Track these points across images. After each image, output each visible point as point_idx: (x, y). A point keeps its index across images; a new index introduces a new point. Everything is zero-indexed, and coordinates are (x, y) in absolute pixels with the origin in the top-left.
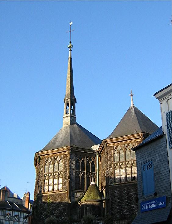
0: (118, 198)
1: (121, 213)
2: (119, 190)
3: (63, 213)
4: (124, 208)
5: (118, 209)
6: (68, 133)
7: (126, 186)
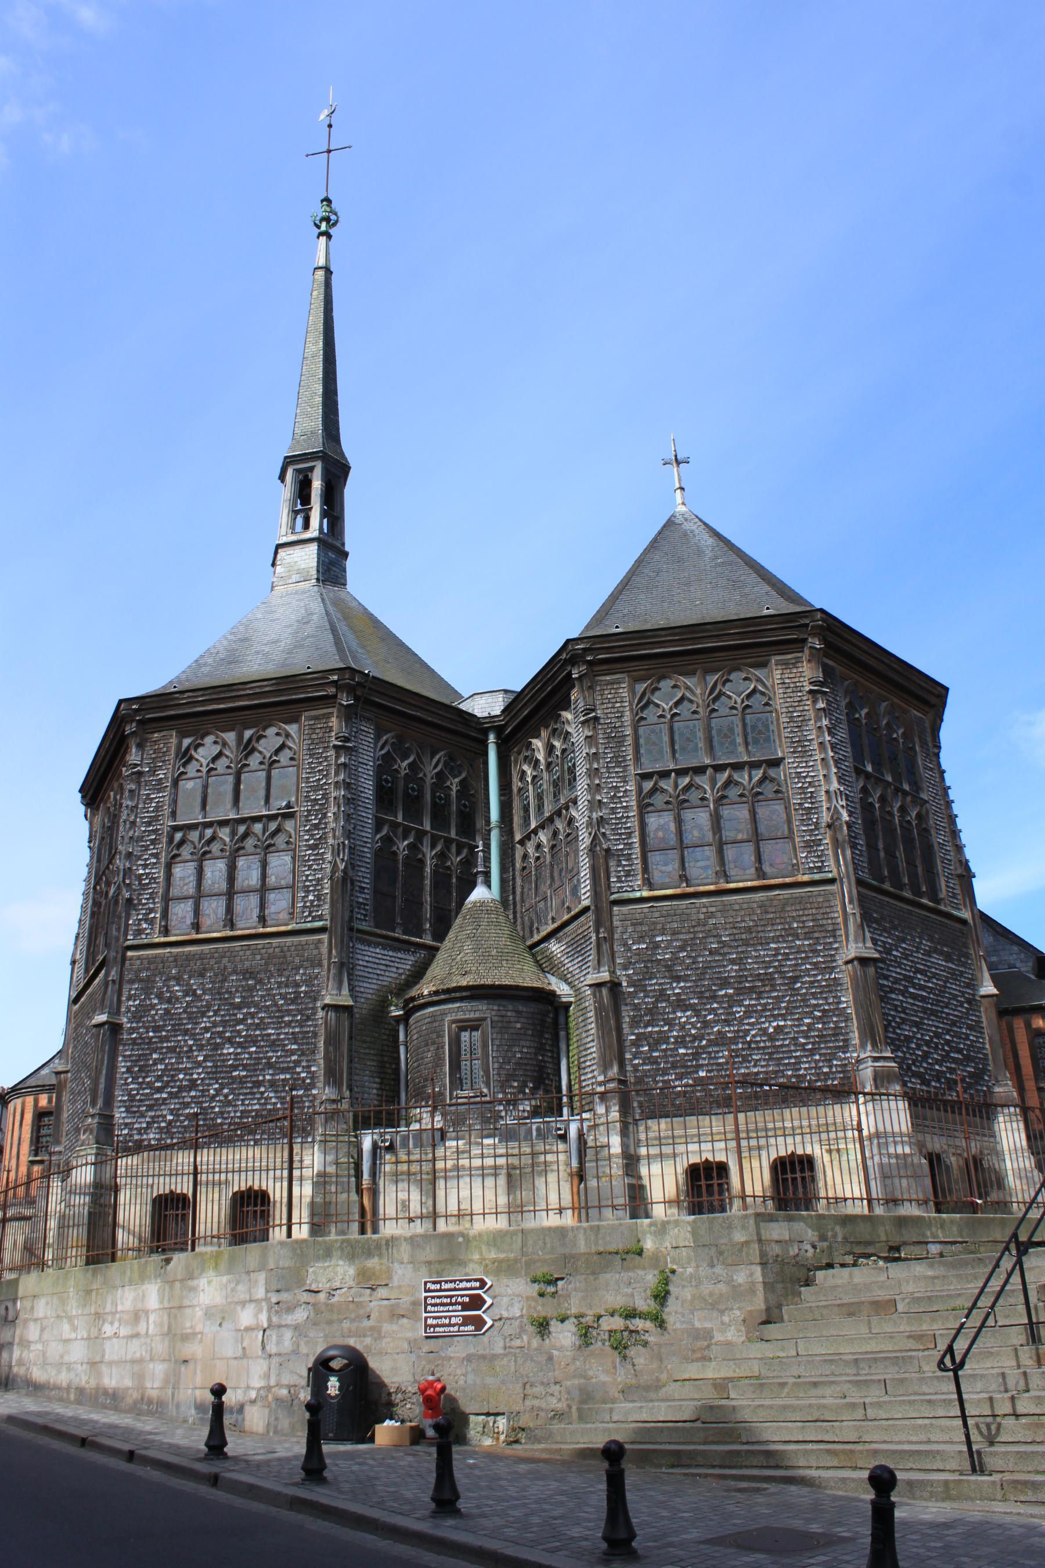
0: (678, 979)
1: (700, 1067)
2: (674, 933)
3: (297, 1063)
4: (721, 1040)
5: (681, 1042)
6: (315, 617)
7: (724, 910)
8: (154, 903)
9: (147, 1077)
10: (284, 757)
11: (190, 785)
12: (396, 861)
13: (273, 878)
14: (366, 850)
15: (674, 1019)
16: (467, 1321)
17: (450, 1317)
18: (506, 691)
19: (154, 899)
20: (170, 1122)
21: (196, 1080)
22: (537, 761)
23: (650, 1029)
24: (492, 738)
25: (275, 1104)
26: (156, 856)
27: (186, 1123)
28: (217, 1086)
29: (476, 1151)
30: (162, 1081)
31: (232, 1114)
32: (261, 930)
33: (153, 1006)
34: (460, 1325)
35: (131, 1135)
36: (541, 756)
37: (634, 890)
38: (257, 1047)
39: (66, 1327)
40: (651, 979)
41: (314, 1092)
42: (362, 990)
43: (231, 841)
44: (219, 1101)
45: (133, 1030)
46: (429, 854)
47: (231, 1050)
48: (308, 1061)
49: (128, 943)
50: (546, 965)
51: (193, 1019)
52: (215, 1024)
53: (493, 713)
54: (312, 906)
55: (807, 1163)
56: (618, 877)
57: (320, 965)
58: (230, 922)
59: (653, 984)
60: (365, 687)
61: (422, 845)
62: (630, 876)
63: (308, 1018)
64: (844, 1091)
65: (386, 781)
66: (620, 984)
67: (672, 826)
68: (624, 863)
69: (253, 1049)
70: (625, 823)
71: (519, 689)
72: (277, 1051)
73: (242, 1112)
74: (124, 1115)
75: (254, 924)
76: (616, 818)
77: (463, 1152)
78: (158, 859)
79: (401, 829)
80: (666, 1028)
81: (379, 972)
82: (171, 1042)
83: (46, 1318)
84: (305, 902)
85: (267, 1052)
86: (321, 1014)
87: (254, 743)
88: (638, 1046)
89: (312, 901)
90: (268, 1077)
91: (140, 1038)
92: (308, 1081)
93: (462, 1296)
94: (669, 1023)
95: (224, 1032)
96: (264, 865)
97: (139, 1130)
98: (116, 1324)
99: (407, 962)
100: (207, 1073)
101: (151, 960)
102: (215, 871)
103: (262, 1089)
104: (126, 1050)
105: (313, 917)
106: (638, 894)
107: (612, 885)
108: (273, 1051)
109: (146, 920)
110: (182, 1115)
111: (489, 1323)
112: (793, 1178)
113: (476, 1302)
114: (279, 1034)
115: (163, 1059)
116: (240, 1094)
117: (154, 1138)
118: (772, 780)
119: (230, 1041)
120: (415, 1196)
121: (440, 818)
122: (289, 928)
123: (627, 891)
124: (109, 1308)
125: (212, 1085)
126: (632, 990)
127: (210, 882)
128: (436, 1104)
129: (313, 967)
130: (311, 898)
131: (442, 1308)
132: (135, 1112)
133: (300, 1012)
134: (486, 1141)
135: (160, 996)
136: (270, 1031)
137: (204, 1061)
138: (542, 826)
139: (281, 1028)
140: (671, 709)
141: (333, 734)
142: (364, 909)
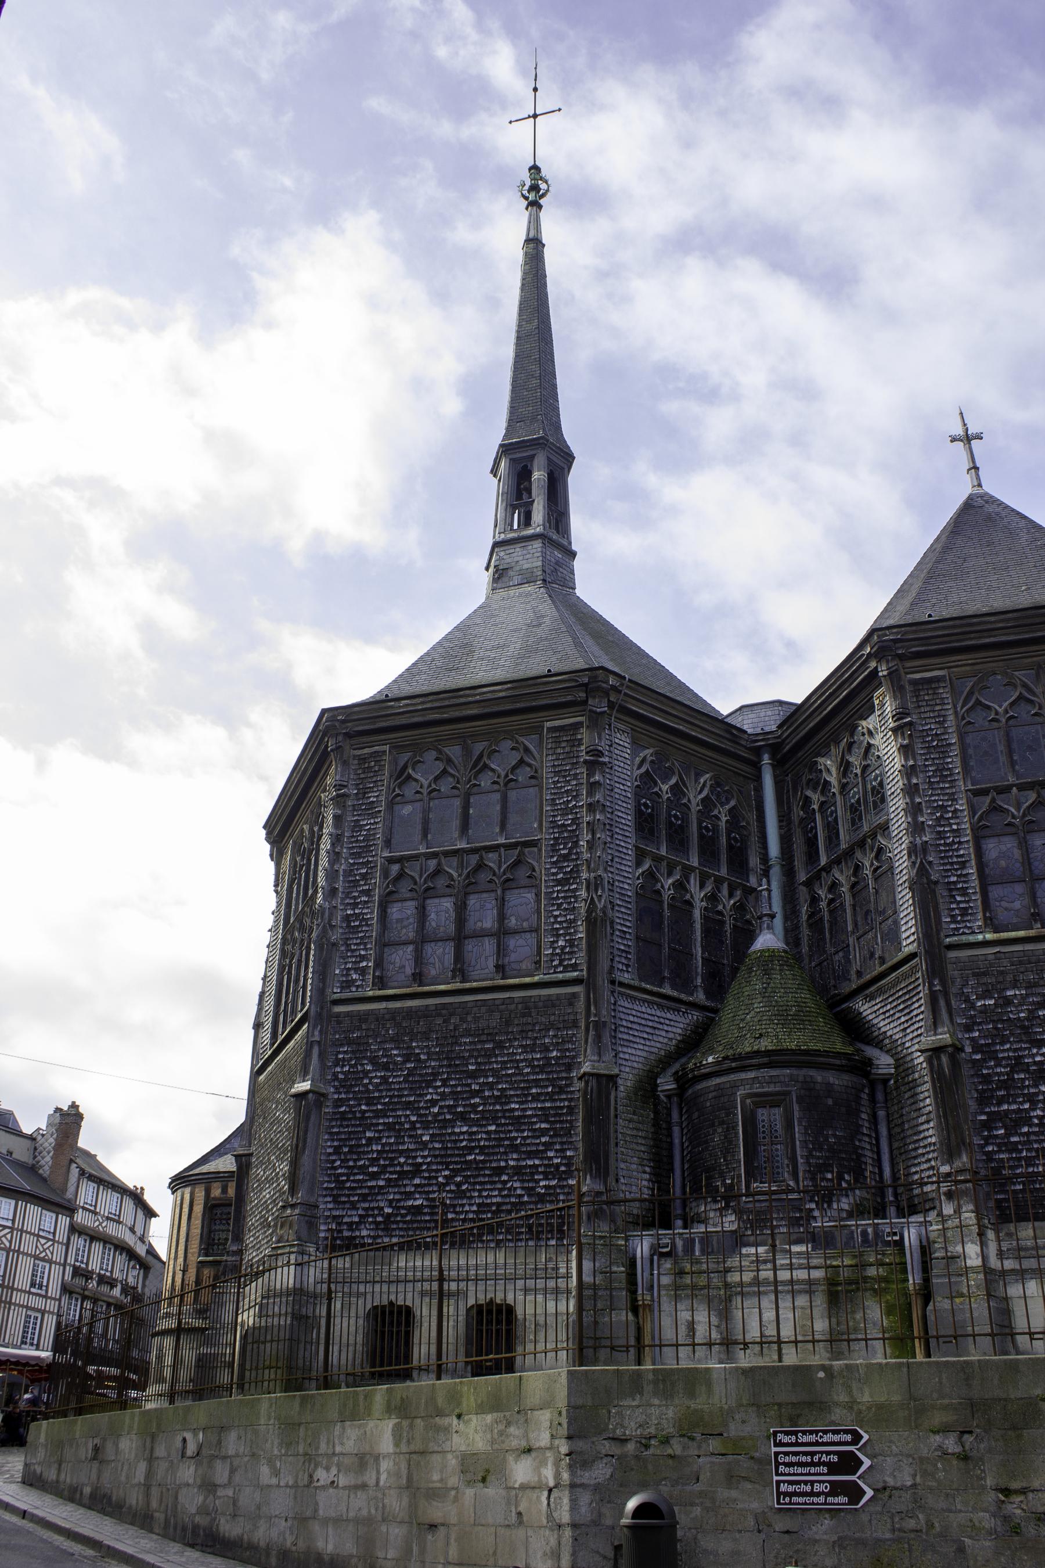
2: (1030, 985)
3: (548, 1146)
8: (366, 949)
9: (360, 1159)
10: (522, 775)
11: (407, 810)
12: (662, 902)
13: (513, 920)
14: (626, 887)
15: (1037, 1094)
16: (836, 1489)
17: (812, 1483)
18: (781, 703)
19: (365, 944)
20: (389, 1215)
21: (421, 1164)
22: (827, 783)
23: (1005, 1107)
24: (766, 759)
25: (521, 1196)
26: (367, 893)
27: (408, 1218)
28: (447, 1173)
29: (782, 1261)
30: (379, 1166)
31: (467, 1208)
32: (502, 982)
33: (366, 1073)
34: (827, 1495)
35: (340, 1231)
36: (833, 779)
37: (973, 933)
38: (498, 1125)
39: (265, 1470)
40: (1002, 1043)
41: (571, 1182)
42: (627, 1057)
43: (460, 875)
44: (451, 1191)
45: (338, 1103)
46: (697, 894)
47: (465, 1129)
48: (562, 1143)
49: (336, 997)
52: (444, 1096)
53: (767, 729)
54: (563, 953)
56: (952, 916)
57: (575, 1024)
58: (460, 970)
59: (1005, 1050)
60: (620, 692)
61: (688, 882)
62: (967, 915)
63: (562, 1090)
65: (645, 805)
66: (962, 1050)
67: (1017, 853)
68: (959, 898)
69: (493, 1128)
70: (958, 850)
71: (799, 701)
72: (523, 1131)
73: (479, 1205)
74: (330, 1206)
75: (491, 976)
76: (945, 844)
77: (765, 1262)
78: (369, 896)
79: (664, 863)
80: (1027, 1106)
81: (645, 1036)
82: (388, 1117)
83: (237, 1455)
84: (554, 949)
85: (510, 1131)
86: (578, 1085)
87: (485, 759)
88: (990, 1129)
89: (563, 948)
90: (512, 1163)
91: (351, 1112)
92: (563, 1168)
93: (828, 1453)
95: (455, 1106)
96: (502, 903)
97: (352, 1223)
98: (334, 1471)
99: (677, 1026)
100: (436, 1156)
101: (363, 1017)
102: (442, 911)
103: (505, 1178)
104: (333, 1127)
105: (565, 967)
106: (980, 937)
107: (945, 926)
108: (517, 1131)
109: (356, 970)
110: (403, 1207)
111: (869, 1493)
113: (848, 1463)
114: (525, 1110)
115: (380, 1138)
116: (475, 1183)
117: (369, 1236)
119: (463, 1117)
120: (702, 1317)
121: (708, 849)
122: (536, 979)
123: (964, 933)
124: (323, 1447)
125: (440, 1171)
126: (978, 1057)
127: (434, 924)
128: (729, 1199)
129: (567, 1028)
130: (561, 943)
131: (800, 1470)
132: (344, 1202)
133: (552, 1082)
134: (796, 1248)
135: (373, 1061)
136: (513, 1106)
137: (431, 1141)
138: (837, 862)
139: (527, 1102)
140: (1006, 711)
141: (583, 748)
142: (626, 958)
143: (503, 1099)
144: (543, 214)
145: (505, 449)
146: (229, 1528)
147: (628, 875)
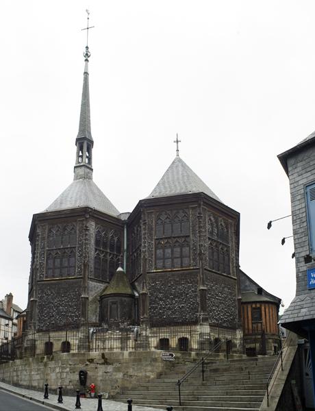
4: (169, 309)
7: (173, 275)
36: (136, 232)
50: (134, 288)
51: (53, 299)
55: (186, 339)
64: (195, 323)
71: (131, 212)
94: (158, 304)
112: (184, 343)
118: (187, 241)
121: (112, 248)
128: (107, 322)
143: (68, 302)
144: (89, 63)
145: (78, 140)
146: (21, 383)
147: (92, 254)
